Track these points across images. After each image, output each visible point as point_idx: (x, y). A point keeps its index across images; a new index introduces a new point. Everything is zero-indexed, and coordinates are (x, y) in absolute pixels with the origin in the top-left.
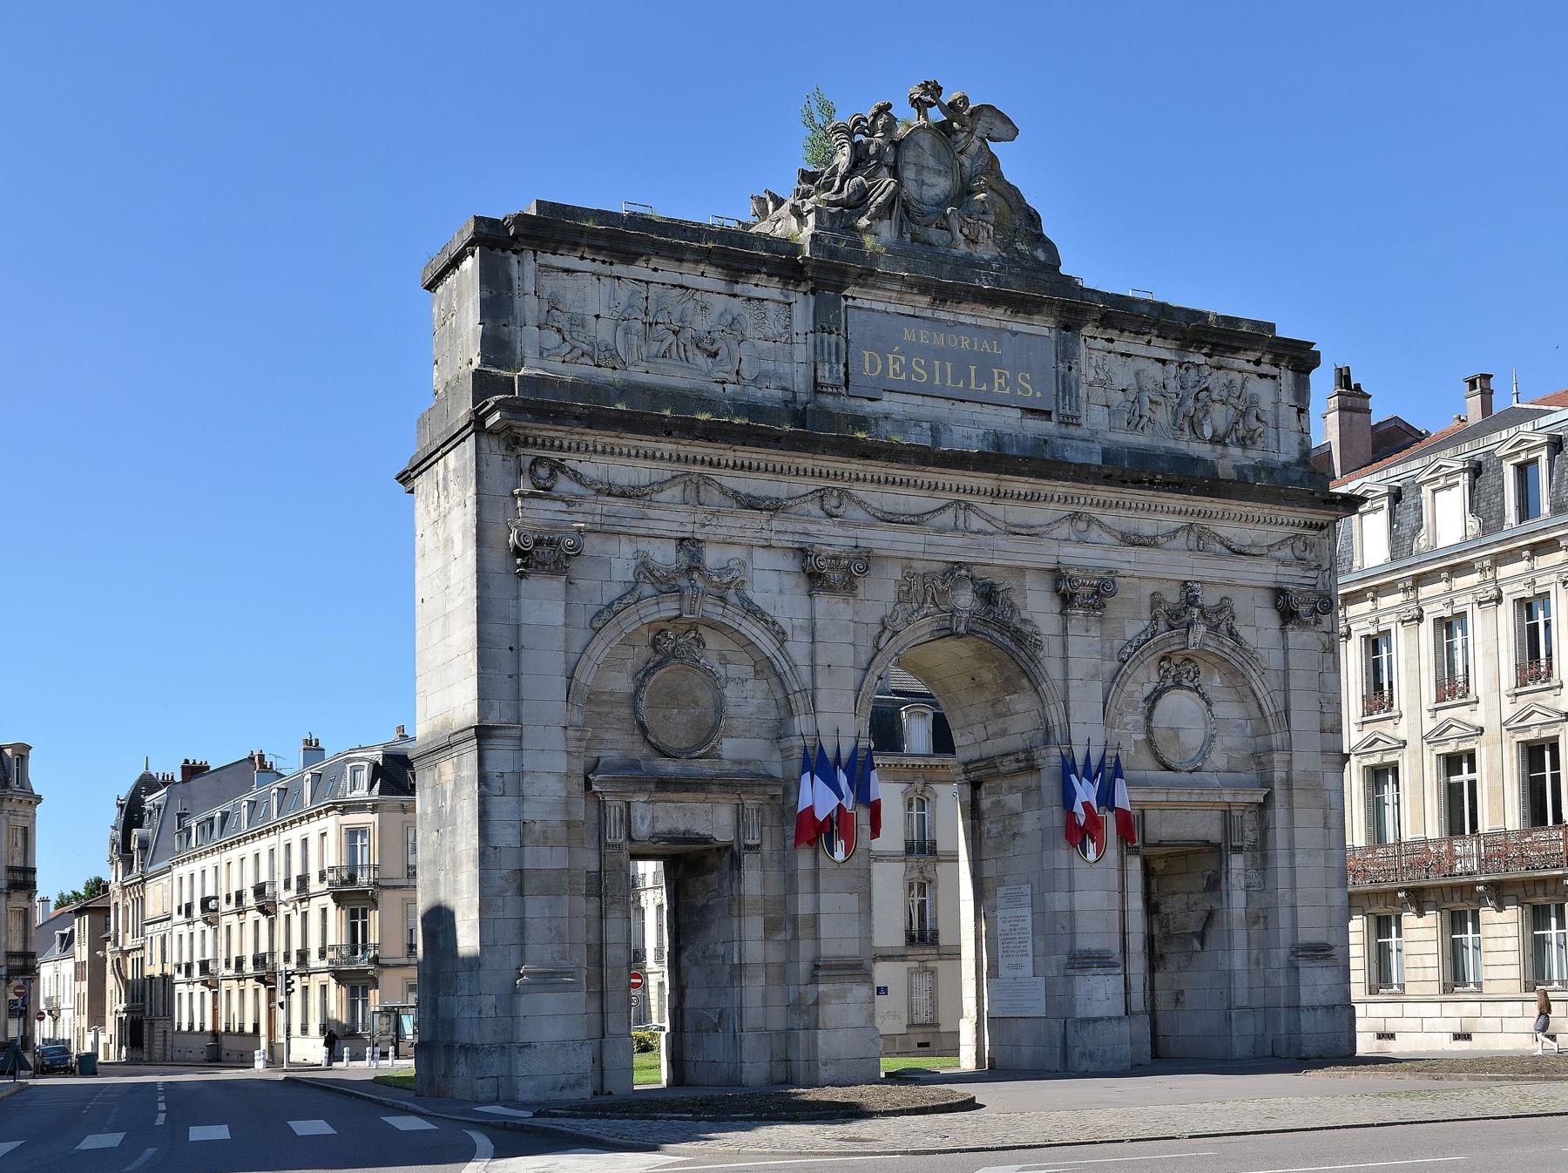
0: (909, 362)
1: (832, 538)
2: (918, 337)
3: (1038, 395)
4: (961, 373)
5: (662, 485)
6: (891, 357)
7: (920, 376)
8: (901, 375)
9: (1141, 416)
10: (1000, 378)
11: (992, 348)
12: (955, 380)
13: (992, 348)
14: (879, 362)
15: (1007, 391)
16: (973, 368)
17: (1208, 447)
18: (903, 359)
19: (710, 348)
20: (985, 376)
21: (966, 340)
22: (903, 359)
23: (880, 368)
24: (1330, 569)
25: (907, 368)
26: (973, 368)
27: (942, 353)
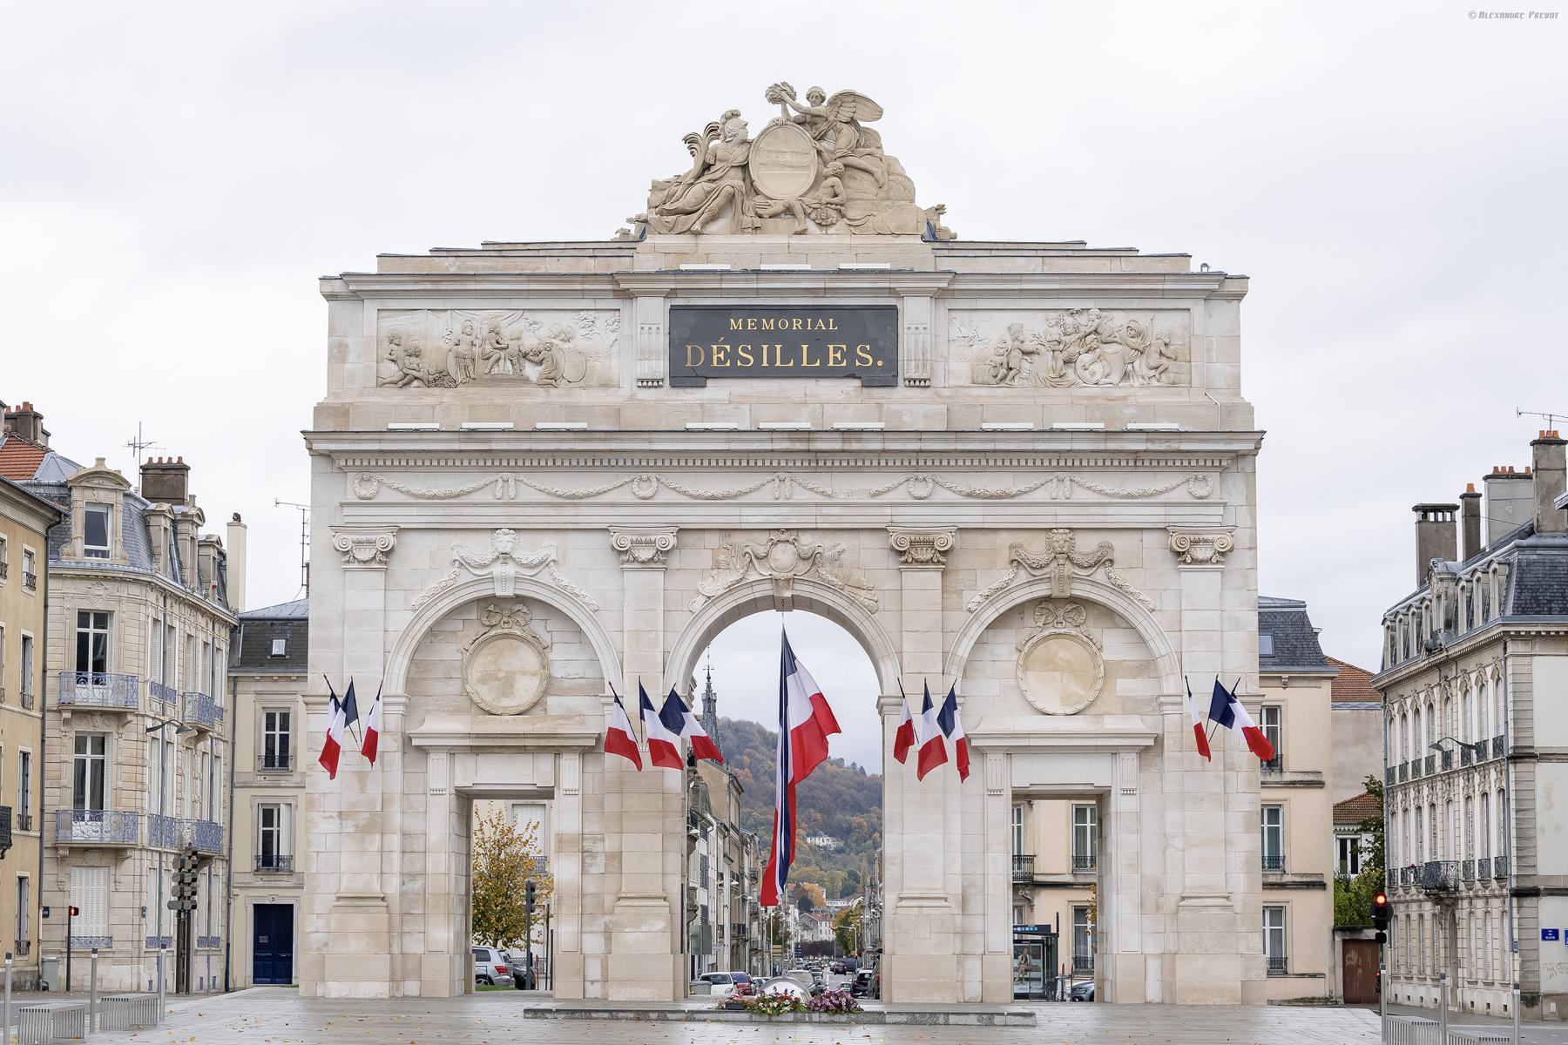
0: (734, 348)
2: (745, 324)
4: (791, 352)
10: (835, 352)
11: (827, 325)
13: (827, 325)
14: (703, 354)
16: (805, 347)
18: (728, 347)
19: (536, 359)
20: (818, 352)
21: (798, 322)
22: (728, 347)
23: (703, 354)
25: (733, 356)
26: (805, 347)
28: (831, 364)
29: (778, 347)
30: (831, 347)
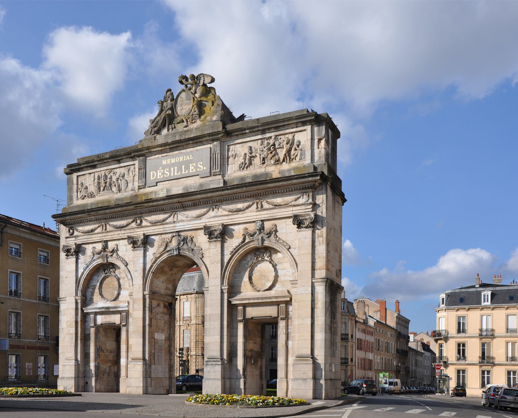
1: (139, 234)
3: (205, 168)
4: (180, 169)
5: (96, 229)
6: (158, 171)
7: (167, 174)
8: (161, 176)
9: (246, 164)
12: (178, 173)
15: (194, 171)
16: (183, 166)
17: (274, 167)
20: (187, 168)
24: (322, 203)
26: (183, 166)
27: (173, 165)
28: (191, 171)
29: (176, 168)
30: (191, 165)
